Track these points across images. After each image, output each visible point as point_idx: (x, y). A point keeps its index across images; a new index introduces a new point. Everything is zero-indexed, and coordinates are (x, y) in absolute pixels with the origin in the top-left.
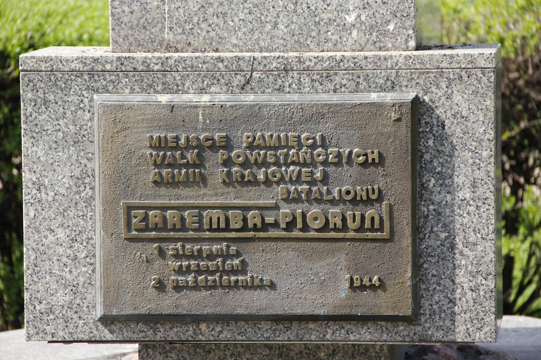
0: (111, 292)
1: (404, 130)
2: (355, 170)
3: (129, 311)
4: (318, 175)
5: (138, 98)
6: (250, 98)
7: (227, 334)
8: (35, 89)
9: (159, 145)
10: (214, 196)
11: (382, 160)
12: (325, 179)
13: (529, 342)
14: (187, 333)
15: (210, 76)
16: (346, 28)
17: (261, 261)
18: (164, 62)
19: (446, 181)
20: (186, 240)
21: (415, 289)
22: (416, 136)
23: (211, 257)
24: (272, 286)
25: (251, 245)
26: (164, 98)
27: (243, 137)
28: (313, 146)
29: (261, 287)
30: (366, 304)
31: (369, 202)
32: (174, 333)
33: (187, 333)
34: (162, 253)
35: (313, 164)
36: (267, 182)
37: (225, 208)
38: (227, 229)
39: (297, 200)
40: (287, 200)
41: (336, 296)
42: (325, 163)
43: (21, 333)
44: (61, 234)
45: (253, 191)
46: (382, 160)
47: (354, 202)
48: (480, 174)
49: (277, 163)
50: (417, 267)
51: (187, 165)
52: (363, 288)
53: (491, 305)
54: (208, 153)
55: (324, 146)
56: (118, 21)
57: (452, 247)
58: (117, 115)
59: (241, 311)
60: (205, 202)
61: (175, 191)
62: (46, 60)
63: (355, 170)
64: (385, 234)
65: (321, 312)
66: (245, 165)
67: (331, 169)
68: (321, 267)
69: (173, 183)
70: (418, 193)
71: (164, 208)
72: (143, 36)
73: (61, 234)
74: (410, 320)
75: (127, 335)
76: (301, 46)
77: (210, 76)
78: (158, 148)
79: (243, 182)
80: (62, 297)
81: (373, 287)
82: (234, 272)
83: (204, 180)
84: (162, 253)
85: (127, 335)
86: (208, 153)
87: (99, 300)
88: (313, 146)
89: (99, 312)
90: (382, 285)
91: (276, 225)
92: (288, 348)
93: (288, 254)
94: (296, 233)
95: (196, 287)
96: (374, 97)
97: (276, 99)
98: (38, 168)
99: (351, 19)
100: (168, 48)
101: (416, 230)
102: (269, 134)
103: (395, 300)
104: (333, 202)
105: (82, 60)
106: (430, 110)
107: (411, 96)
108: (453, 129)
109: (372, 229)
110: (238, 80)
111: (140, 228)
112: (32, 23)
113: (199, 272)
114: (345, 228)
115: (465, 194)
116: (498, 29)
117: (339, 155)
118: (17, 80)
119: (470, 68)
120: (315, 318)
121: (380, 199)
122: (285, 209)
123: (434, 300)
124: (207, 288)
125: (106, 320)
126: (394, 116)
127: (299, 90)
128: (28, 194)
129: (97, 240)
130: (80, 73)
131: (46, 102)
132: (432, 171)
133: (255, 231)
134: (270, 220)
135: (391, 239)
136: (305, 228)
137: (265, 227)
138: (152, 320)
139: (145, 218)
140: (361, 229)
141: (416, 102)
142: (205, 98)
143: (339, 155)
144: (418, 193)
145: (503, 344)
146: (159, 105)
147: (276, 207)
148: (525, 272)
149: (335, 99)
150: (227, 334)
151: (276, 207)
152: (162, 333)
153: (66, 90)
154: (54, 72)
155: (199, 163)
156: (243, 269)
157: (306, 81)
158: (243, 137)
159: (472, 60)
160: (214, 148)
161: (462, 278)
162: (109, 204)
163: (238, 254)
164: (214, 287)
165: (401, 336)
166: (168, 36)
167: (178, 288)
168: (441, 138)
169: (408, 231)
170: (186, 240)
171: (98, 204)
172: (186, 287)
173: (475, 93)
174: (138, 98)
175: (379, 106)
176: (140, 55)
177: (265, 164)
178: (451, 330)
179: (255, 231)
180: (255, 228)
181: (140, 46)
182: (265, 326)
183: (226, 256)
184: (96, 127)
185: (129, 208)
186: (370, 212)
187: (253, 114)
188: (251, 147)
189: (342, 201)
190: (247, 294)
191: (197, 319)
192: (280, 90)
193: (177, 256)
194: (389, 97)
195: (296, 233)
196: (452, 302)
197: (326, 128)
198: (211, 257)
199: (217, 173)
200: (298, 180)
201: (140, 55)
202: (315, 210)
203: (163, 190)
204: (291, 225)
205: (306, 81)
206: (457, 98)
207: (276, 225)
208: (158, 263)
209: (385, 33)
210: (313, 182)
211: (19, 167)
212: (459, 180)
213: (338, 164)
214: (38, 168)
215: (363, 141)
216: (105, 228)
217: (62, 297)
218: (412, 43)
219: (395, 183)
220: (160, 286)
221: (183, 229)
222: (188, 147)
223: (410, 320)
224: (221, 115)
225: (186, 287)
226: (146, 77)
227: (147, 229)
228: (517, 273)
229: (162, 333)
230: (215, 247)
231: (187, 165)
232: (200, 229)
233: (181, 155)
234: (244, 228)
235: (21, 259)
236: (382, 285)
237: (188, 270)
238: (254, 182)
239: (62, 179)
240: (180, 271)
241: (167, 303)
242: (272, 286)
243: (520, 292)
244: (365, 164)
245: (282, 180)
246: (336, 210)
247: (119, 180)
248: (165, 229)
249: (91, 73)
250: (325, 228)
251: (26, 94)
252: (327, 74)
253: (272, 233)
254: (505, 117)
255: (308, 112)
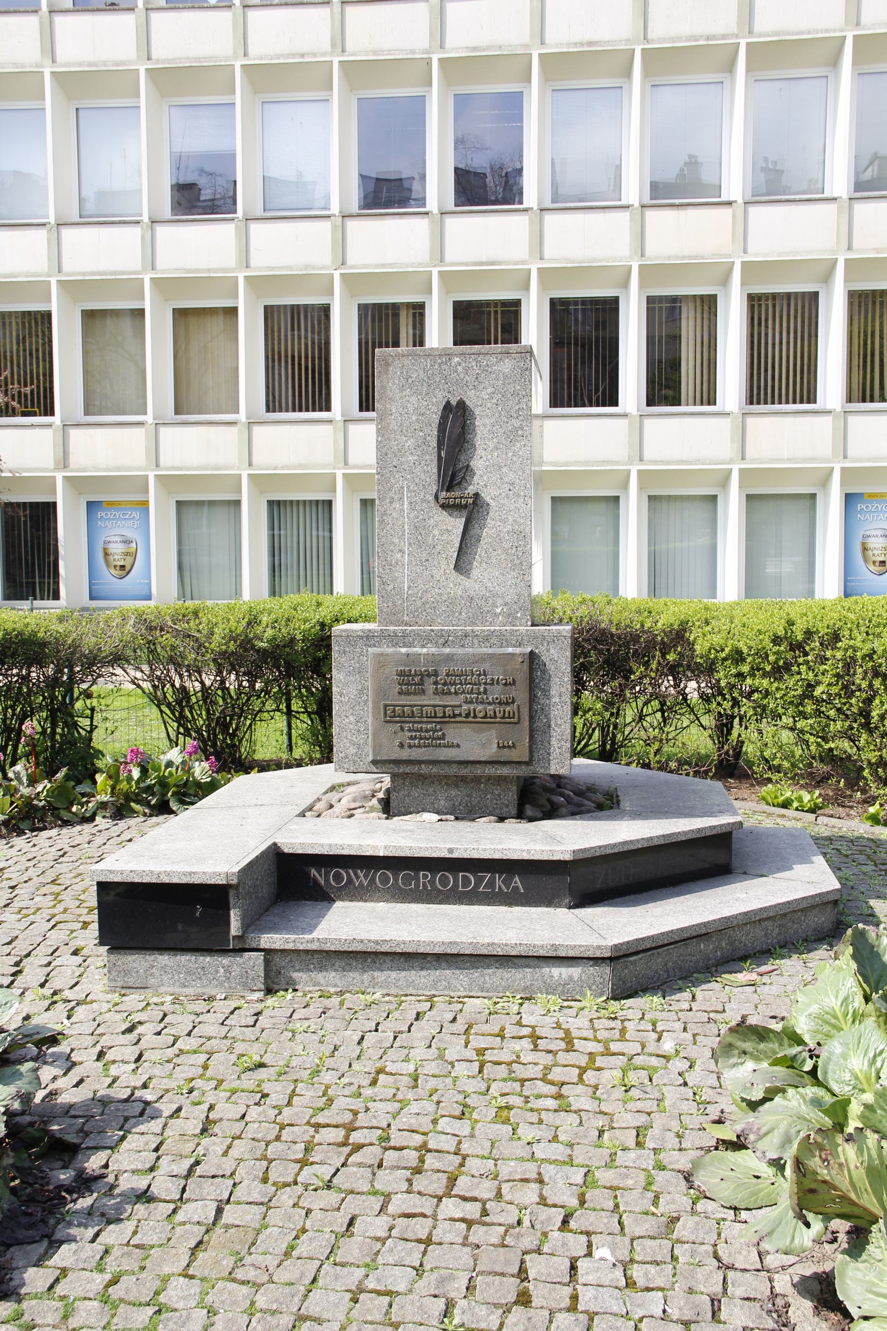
0: (377, 748)
1: (526, 666)
2: (500, 687)
3: (386, 758)
4: (482, 690)
5: (391, 650)
6: (447, 650)
7: (435, 770)
8: (339, 645)
9: (401, 674)
10: (429, 700)
11: (514, 682)
12: (485, 692)
13: (585, 772)
14: (415, 769)
15: (426, 639)
16: (496, 615)
17: (452, 733)
18: (404, 632)
19: (546, 693)
20: (414, 722)
21: (531, 747)
22: (531, 670)
23: (427, 731)
24: (458, 746)
25: (448, 725)
26: (404, 650)
27: (443, 670)
28: (479, 675)
29: (453, 746)
30: (506, 755)
31: (507, 703)
32: (408, 769)
33: (415, 769)
34: (402, 729)
35: (480, 684)
36: (456, 693)
37: (434, 706)
38: (435, 717)
39: (471, 702)
40: (466, 702)
41: (490, 751)
42: (485, 683)
43: (330, 767)
44: (352, 719)
45: (448, 698)
46: (514, 682)
47: (500, 703)
48: (563, 690)
49: (461, 684)
50: (531, 737)
51: (415, 684)
52: (504, 747)
53: (568, 755)
54: (426, 678)
55: (485, 675)
56: (381, 611)
57: (549, 726)
58: (381, 661)
59: (442, 758)
60: (424, 703)
61: (409, 698)
62: (345, 631)
63: (500, 687)
64: (515, 720)
65: (483, 759)
66: (445, 684)
67: (488, 687)
68: (483, 737)
69: (408, 693)
70: (532, 699)
71: (403, 706)
72: (393, 618)
73: (352, 719)
74: (528, 763)
75: (385, 770)
76: (473, 624)
77: (426, 639)
78: (400, 675)
79: (443, 693)
80: (352, 750)
81: (509, 747)
82: (439, 739)
83: (423, 692)
84: (402, 729)
85: (385, 770)
86: (426, 678)
87: (371, 752)
88: (479, 675)
89: (371, 758)
90: (514, 746)
91: (460, 715)
92: (466, 777)
93: (466, 730)
94: (470, 719)
95: (419, 746)
96: (510, 650)
97: (460, 651)
98: (340, 685)
99: (498, 610)
100: (406, 625)
101: (531, 718)
102: (456, 668)
103: (521, 753)
104: (489, 704)
105: (363, 631)
106: (539, 657)
107: (529, 649)
108: (550, 667)
109: (509, 717)
110: (441, 641)
111: (392, 716)
112: (337, 608)
113: (421, 739)
114: (495, 717)
115: (556, 699)
116: (569, 612)
117: (492, 680)
118: (330, 636)
119: (558, 636)
120: (480, 762)
121: (513, 702)
122: (465, 707)
123: (539, 754)
124: (425, 747)
125: (374, 762)
126: (520, 660)
127: (472, 647)
128: (335, 699)
129: (370, 722)
130: (362, 637)
131: (345, 652)
132: (540, 688)
133: (449, 718)
134: (457, 712)
135: (518, 723)
136: (475, 716)
137: (455, 716)
138: (397, 762)
139: (394, 711)
140: (503, 717)
141: (532, 652)
142: (425, 650)
143: (492, 680)
144: (532, 699)
145: (575, 772)
146: (402, 654)
147: (460, 706)
148: (581, 734)
149: (491, 651)
150: (435, 770)
151: (460, 706)
152: (402, 769)
153: (355, 646)
154: (349, 637)
155: (421, 683)
156: (443, 737)
157: (476, 641)
158: (443, 670)
159: (559, 632)
160: (429, 675)
161: (554, 742)
162: (375, 703)
163: (441, 730)
164: (429, 746)
165: (523, 771)
166: (406, 618)
167: (410, 747)
168: (544, 671)
169: (527, 718)
170: (414, 722)
171: (370, 703)
172: (414, 746)
173: (561, 648)
174: (391, 650)
175: (513, 655)
176: (392, 628)
177: (455, 684)
178: (548, 768)
179: (449, 718)
180: (449, 717)
181: (392, 623)
182: (454, 766)
183: (435, 731)
184: (370, 665)
185: (386, 706)
186: (508, 709)
187: (449, 658)
188: (448, 675)
189: (494, 703)
190: (445, 750)
191: (420, 762)
192: (463, 646)
193: (410, 730)
194: (518, 650)
195: (470, 719)
196: (549, 754)
197: (486, 666)
198: (427, 731)
199: (430, 688)
200: (472, 692)
201: (392, 628)
202: (480, 707)
203: (403, 697)
204: (468, 715)
205: (476, 641)
206: (552, 651)
207: (460, 715)
208: (400, 734)
209: (516, 618)
210: (479, 693)
211: (330, 679)
212: (553, 692)
213: (492, 684)
214: (340, 685)
215: (505, 673)
216: (374, 716)
217: (352, 750)
218: (529, 623)
219: (520, 694)
220: (401, 745)
221: (413, 716)
222: (416, 675)
223: (528, 763)
224: (432, 659)
225: (414, 746)
226: (394, 639)
227: (394, 716)
228: (577, 734)
229: (402, 769)
230: (429, 726)
231: (415, 684)
232: (422, 717)
233: (412, 679)
234: (444, 716)
235: (331, 724)
236: (514, 746)
237: (416, 738)
238: (449, 693)
239: (353, 691)
240: (411, 738)
241: (405, 754)
242: (458, 746)
243: (579, 743)
244: (505, 684)
245: (463, 692)
246: (491, 707)
247: (381, 692)
248: (404, 716)
249: (367, 637)
250: (485, 717)
251: (335, 648)
252: (486, 639)
253: (458, 719)
254: (575, 657)
255: (477, 658)
